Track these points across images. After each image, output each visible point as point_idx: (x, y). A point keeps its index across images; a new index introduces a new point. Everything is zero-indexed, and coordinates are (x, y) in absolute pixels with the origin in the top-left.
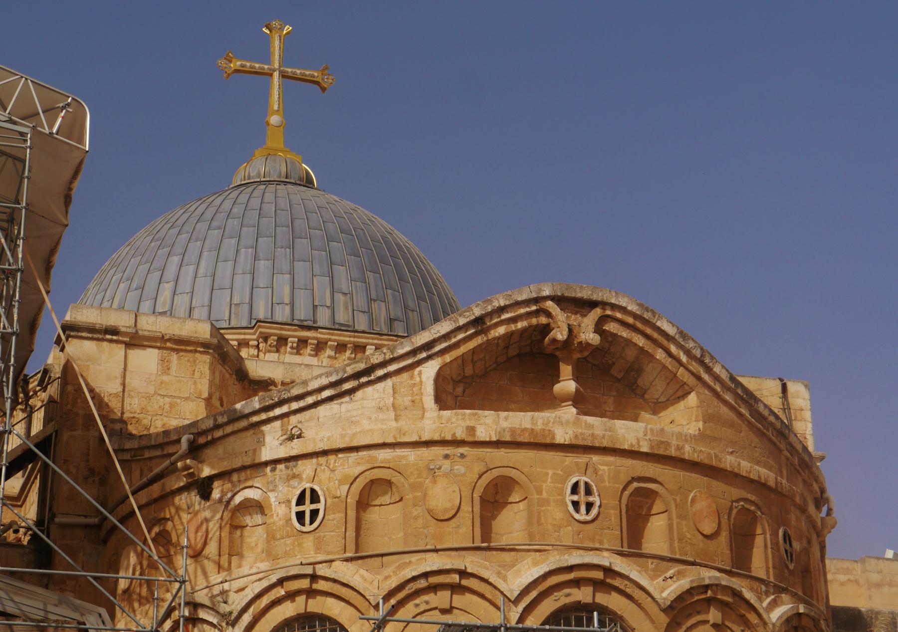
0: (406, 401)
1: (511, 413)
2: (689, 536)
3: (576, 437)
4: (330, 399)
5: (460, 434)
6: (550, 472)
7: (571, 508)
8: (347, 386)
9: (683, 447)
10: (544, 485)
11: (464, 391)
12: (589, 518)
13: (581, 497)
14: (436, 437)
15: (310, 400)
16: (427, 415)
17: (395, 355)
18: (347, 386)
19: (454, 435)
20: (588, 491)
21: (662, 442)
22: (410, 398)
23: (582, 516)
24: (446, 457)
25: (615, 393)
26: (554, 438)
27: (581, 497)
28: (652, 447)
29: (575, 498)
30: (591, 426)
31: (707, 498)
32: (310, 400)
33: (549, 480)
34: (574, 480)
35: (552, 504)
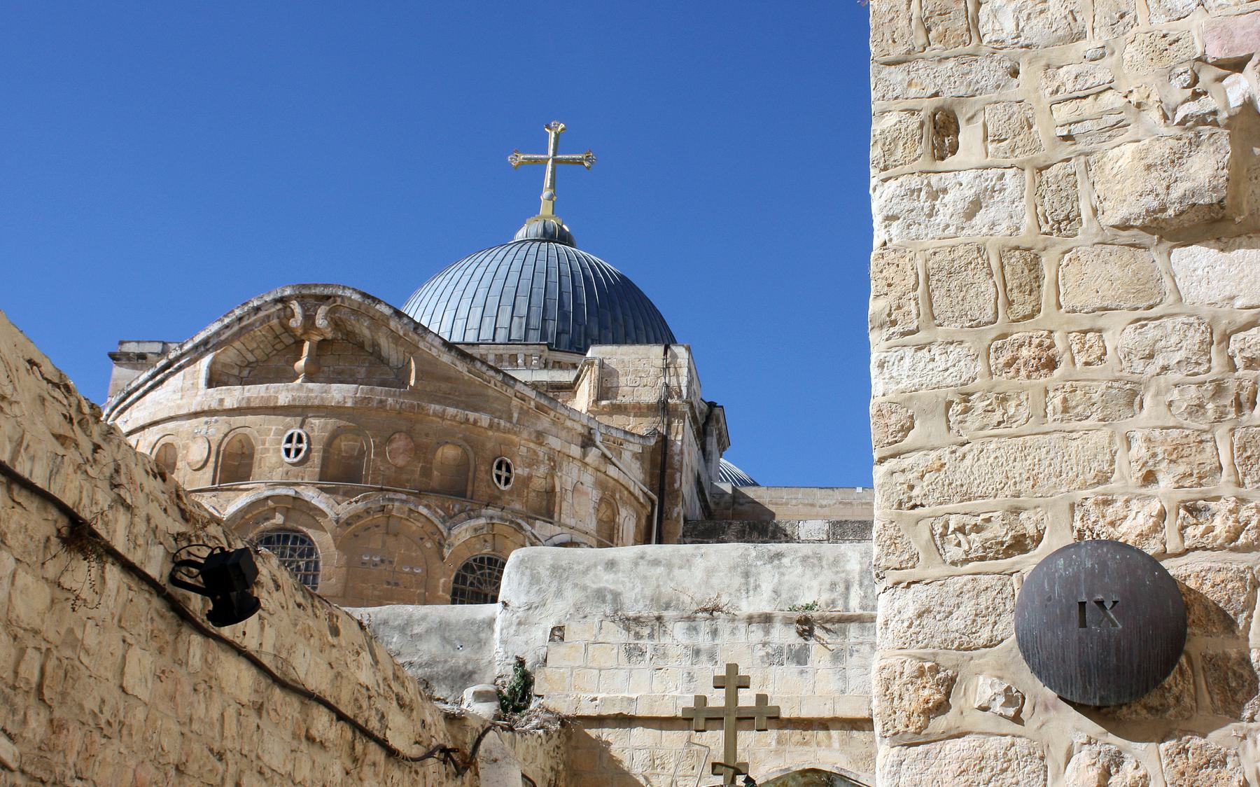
0: (188, 383)
1: (253, 386)
2: (382, 468)
3: (294, 400)
4: (152, 388)
5: (214, 405)
6: (274, 428)
7: (283, 453)
8: (158, 378)
9: (386, 400)
10: (268, 438)
11: (249, 373)
12: (296, 460)
13: (293, 446)
14: (199, 409)
15: (141, 391)
16: (199, 393)
17: (183, 351)
18: (158, 378)
19: (209, 406)
20: (300, 440)
21: (365, 398)
22: (191, 382)
23: (292, 459)
24: (206, 423)
25: (367, 365)
26: (277, 402)
27: (293, 446)
28: (356, 403)
29: (288, 446)
30: (311, 390)
31: (406, 439)
32: (141, 391)
33: (272, 434)
34: (289, 433)
35: (271, 451)
